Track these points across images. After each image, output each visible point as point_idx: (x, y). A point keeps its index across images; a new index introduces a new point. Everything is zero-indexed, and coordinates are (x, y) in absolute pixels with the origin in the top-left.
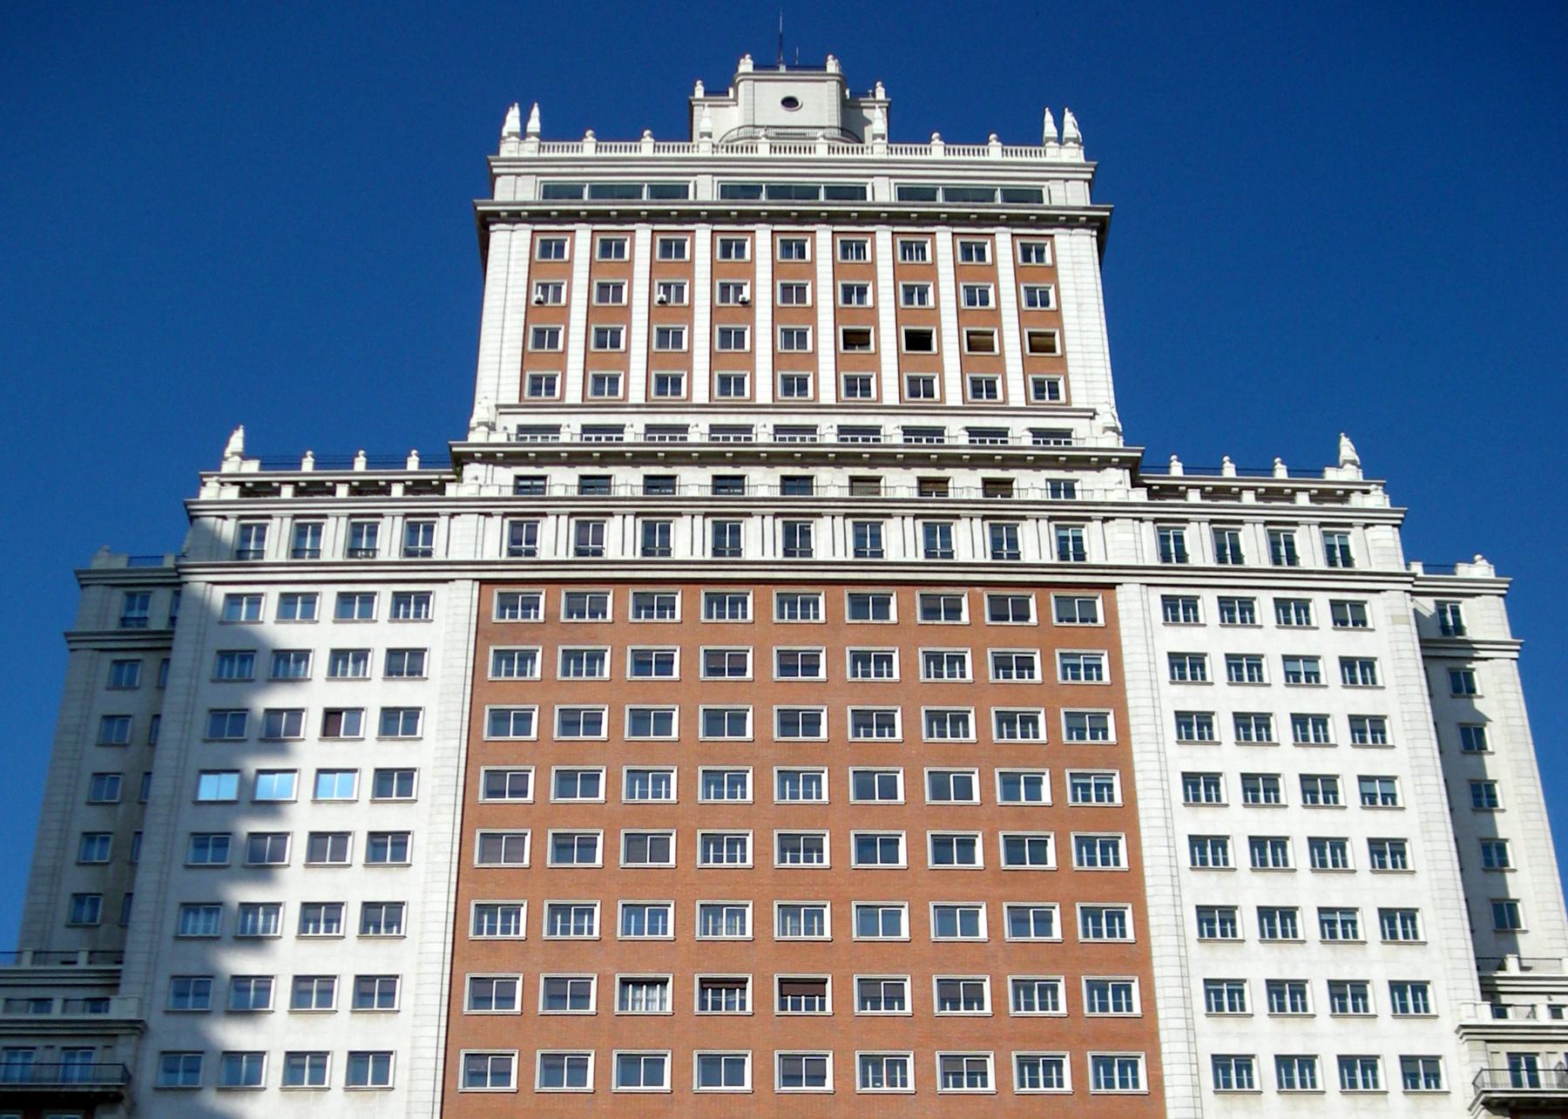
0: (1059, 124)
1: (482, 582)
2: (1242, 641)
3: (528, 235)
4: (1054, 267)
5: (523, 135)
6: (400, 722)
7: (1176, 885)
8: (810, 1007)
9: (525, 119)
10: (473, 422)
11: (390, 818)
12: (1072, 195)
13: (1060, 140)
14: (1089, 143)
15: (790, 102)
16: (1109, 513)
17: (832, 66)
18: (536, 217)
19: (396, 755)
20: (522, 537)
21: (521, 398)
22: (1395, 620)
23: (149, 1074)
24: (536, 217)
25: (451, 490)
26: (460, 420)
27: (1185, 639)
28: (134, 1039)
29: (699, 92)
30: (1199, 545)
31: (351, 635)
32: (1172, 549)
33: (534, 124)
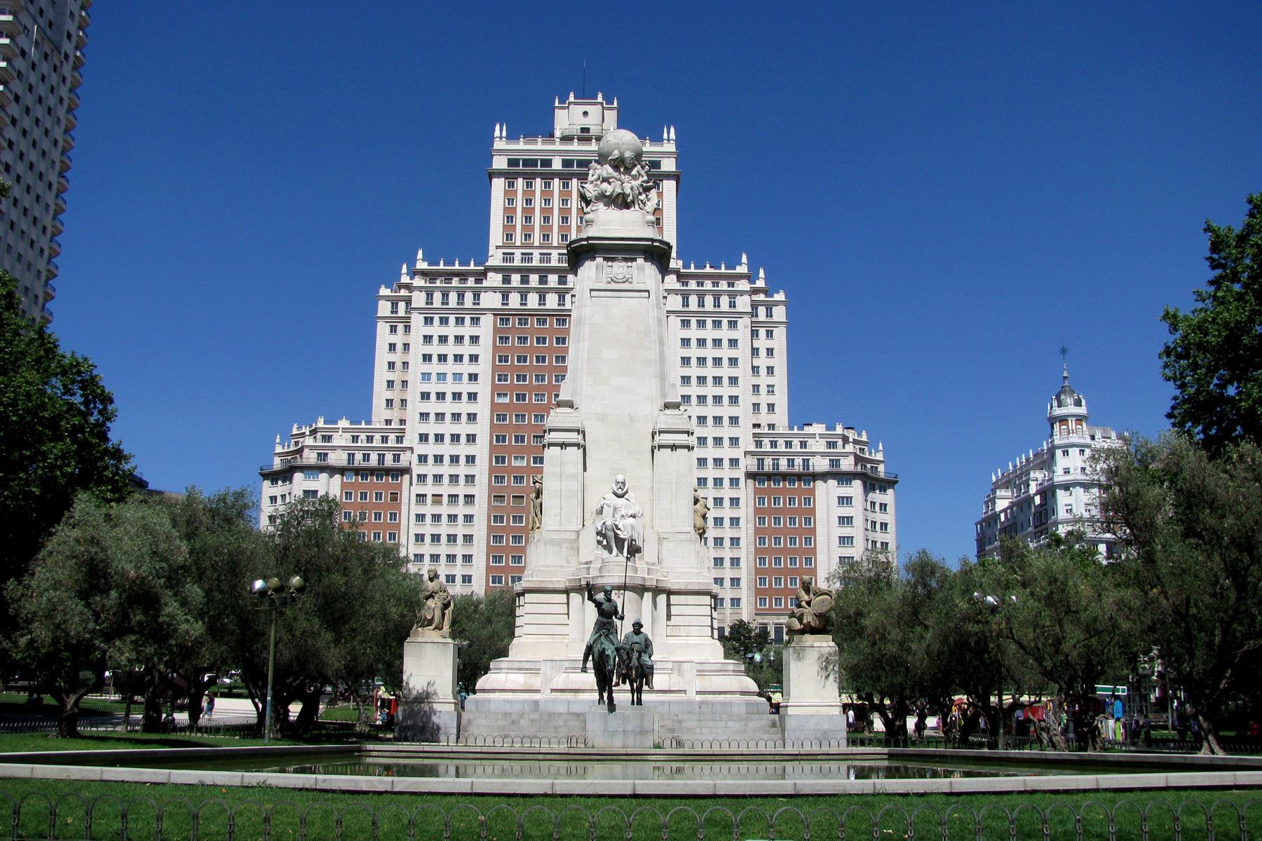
0: (669, 133)
1: (494, 314)
4: (662, 192)
5: (501, 138)
6: (474, 358)
9: (501, 131)
10: (490, 254)
11: (473, 388)
12: (669, 165)
13: (669, 140)
14: (678, 142)
15: (585, 113)
17: (600, 99)
19: (473, 369)
20: (505, 297)
22: (746, 327)
25: (485, 284)
26: (486, 257)
27: (686, 334)
29: (557, 104)
30: (693, 300)
31: (460, 331)
32: (686, 303)
33: (504, 134)
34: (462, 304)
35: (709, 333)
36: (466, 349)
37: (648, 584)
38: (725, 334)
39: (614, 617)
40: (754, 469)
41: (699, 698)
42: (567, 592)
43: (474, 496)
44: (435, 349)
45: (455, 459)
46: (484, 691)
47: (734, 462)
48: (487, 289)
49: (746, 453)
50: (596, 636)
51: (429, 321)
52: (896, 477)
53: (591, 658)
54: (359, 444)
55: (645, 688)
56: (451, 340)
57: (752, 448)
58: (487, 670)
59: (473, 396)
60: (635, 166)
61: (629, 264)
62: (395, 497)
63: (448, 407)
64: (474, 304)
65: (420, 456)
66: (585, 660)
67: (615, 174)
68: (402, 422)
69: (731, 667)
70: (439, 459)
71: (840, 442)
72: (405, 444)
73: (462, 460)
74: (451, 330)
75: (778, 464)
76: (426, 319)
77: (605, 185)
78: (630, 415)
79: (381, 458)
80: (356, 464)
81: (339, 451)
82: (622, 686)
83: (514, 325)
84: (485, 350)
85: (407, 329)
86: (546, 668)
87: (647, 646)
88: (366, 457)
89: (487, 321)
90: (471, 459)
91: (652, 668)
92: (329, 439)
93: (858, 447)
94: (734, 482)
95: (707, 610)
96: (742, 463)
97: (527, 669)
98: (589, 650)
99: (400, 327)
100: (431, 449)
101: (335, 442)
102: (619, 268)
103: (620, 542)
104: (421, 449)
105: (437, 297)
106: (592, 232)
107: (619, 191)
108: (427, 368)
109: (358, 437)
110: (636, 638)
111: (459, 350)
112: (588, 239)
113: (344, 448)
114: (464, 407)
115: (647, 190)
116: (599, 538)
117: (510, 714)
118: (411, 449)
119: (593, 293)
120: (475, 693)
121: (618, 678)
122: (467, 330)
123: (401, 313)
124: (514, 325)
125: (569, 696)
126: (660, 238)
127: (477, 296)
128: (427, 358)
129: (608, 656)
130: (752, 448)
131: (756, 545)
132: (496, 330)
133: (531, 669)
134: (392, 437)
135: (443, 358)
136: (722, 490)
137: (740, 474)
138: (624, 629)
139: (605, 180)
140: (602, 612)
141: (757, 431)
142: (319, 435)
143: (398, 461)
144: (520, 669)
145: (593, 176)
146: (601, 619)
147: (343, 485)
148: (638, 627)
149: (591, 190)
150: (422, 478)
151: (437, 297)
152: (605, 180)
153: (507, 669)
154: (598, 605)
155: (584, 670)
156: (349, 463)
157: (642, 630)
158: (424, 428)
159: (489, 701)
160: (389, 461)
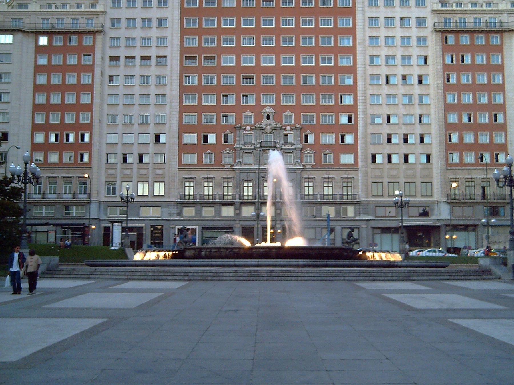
8: (270, 5)
23: (108, 25)
28: (103, 15)
40: (442, 27)
43: (166, 57)
47: (421, 22)
49: (434, 11)
57: (439, 7)
75: (465, 23)
92: (26, 6)
94: (422, 40)
96: (430, 23)
113: (36, 13)
118: (104, 12)
130: (439, 7)
131: (445, 101)
136: (410, 49)
137: (427, 32)
160: (82, 24)
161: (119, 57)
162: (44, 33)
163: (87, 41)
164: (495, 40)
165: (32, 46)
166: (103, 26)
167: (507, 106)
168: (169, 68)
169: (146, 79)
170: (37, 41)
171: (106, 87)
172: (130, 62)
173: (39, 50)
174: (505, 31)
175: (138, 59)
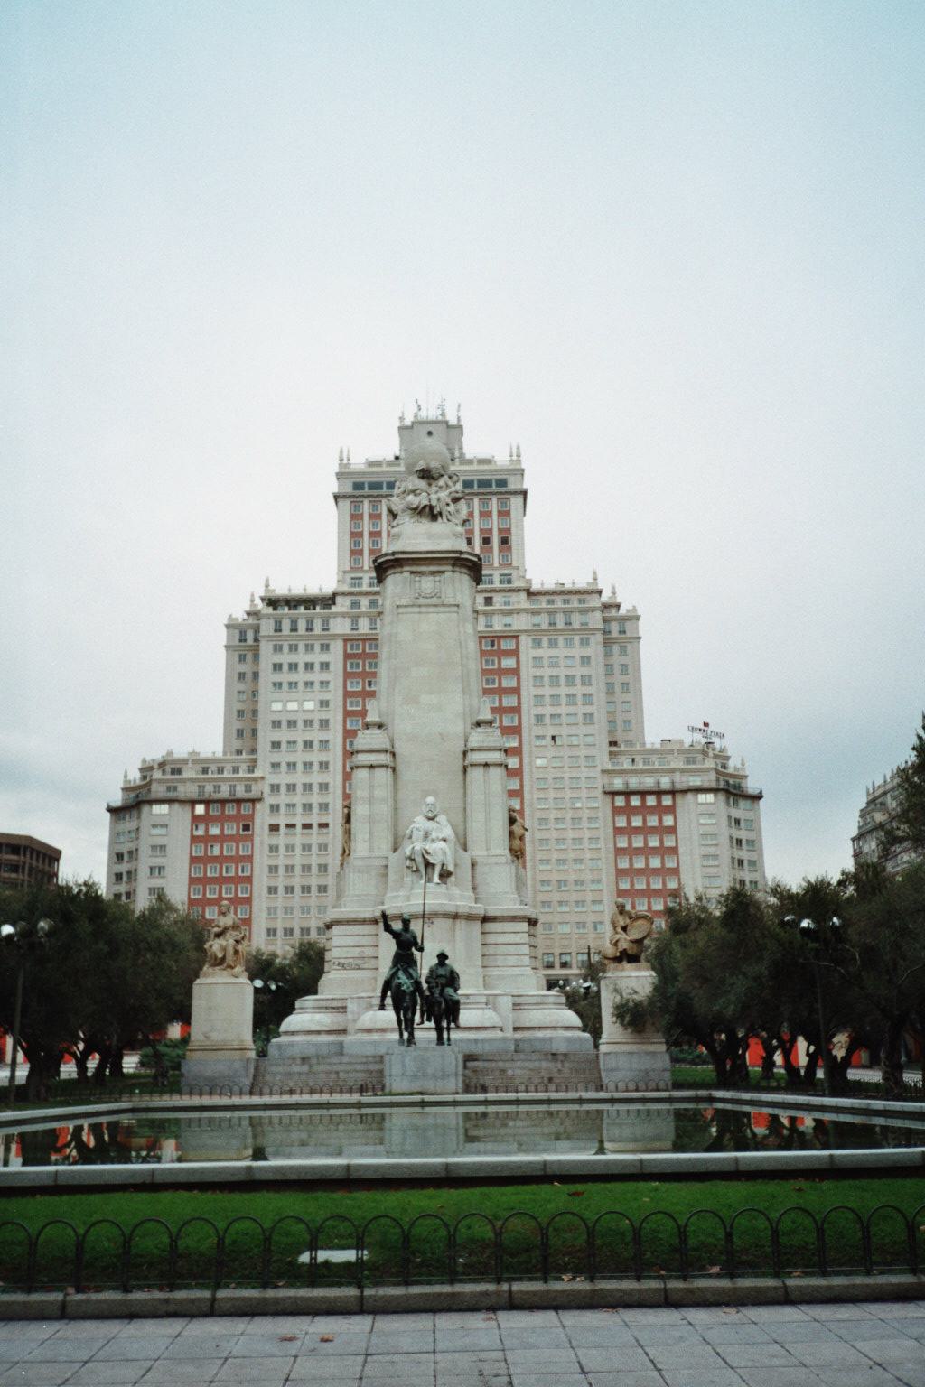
2: (554, 652)
3: (349, 502)
7: (530, 730)
15: (430, 433)
16: (518, 611)
18: (350, 496)
19: (325, 696)
20: (355, 619)
21: (352, 568)
22: (597, 643)
24: (350, 496)
25: (334, 609)
31: (309, 658)
34: (312, 630)
35: (561, 652)
36: (316, 676)
37: (460, 911)
38: (577, 652)
39: (413, 949)
41: (519, 1035)
42: (375, 922)
44: (285, 677)
45: (308, 787)
46: (286, 1033)
48: (336, 615)
49: (603, 772)
50: (394, 970)
51: (278, 649)
52: (761, 792)
53: (389, 994)
54: (210, 775)
55: (452, 1025)
56: (301, 667)
58: (290, 1009)
59: (325, 724)
60: (442, 476)
61: (437, 578)
62: (246, 827)
63: (300, 735)
64: (324, 630)
65: (272, 786)
66: (383, 996)
67: (422, 484)
68: (254, 751)
69: (551, 1000)
70: (291, 788)
71: (700, 757)
72: (257, 773)
73: (316, 788)
74: (301, 658)
76: (275, 646)
77: (410, 498)
78: (440, 734)
79: (233, 787)
80: (206, 797)
81: (188, 784)
82: (427, 1024)
83: (364, 650)
84: (335, 676)
85: (256, 657)
86: (351, 1006)
87: (452, 980)
88: (217, 789)
89: (337, 648)
90: (324, 787)
91: (457, 1002)
92: (179, 771)
93: (718, 761)
95: (525, 938)
97: (334, 1008)
98: (387, 985)
99: (249, 656)
100: (283, 778)
101: (185, 775)
102: (427, 584)
103: (428, 865)
104: (274, 779)
105: (286, 625)
106: (397, 546)
107: (426, 503)
108: (276, 695)
109: (208, 768)
110: (442, 971)
111: (310, 677)
112: (393, 553)
113: (192, 780)
114: (315, 735)
115: (456, 500)
116: (408, 863)
117: (309, 1058)
118: (262, 778)
119: (401, 610)
120: (280, 1036)
121: (422, 1016)
122: (317, 657)
123: (250, 641)
124: (364, 650)
125: (375, 1036)
126: (469, 550)
127: (326, 622)
128: (277, 685)
129: (404, 991)
130: (609, 767)
132: (347, 656)
133: (338, 1008)
134: (243, 767)
135: (293, 685)
137: (598, 793)
138: (426, 962)
139: (414, 492)
140: (399, 944)
141: (614, 749)
142: (168, 768)
143: (250, 791)
144: (326, 1008)
145: (399, 488)
146: (400, 951)
147: (196, 819)
148: (442, 957)
149: (397, 503)
150: (275, 808)
151: (286, 625)
152: (414, 492)
153: (314, 1008)
154: (396, 935)
155: (382, 1007)
156: (199, 795)
157: (447, 962)
158: (276, 758)
159: (292, 1044)
160: (240, 792)
161: (278, 825)
162: (200, 802)
163: (245, 809)
164: (667, 801)
165: (188, 816)
166: (262, 793)
167: (681, 871)
168: (331, 835)
169: (306, 848)
170: (193, 810)
171: (266, 858)
172: (291, 831)
173: (196, 819)
174: (677, 791)
175: (299, 827)
